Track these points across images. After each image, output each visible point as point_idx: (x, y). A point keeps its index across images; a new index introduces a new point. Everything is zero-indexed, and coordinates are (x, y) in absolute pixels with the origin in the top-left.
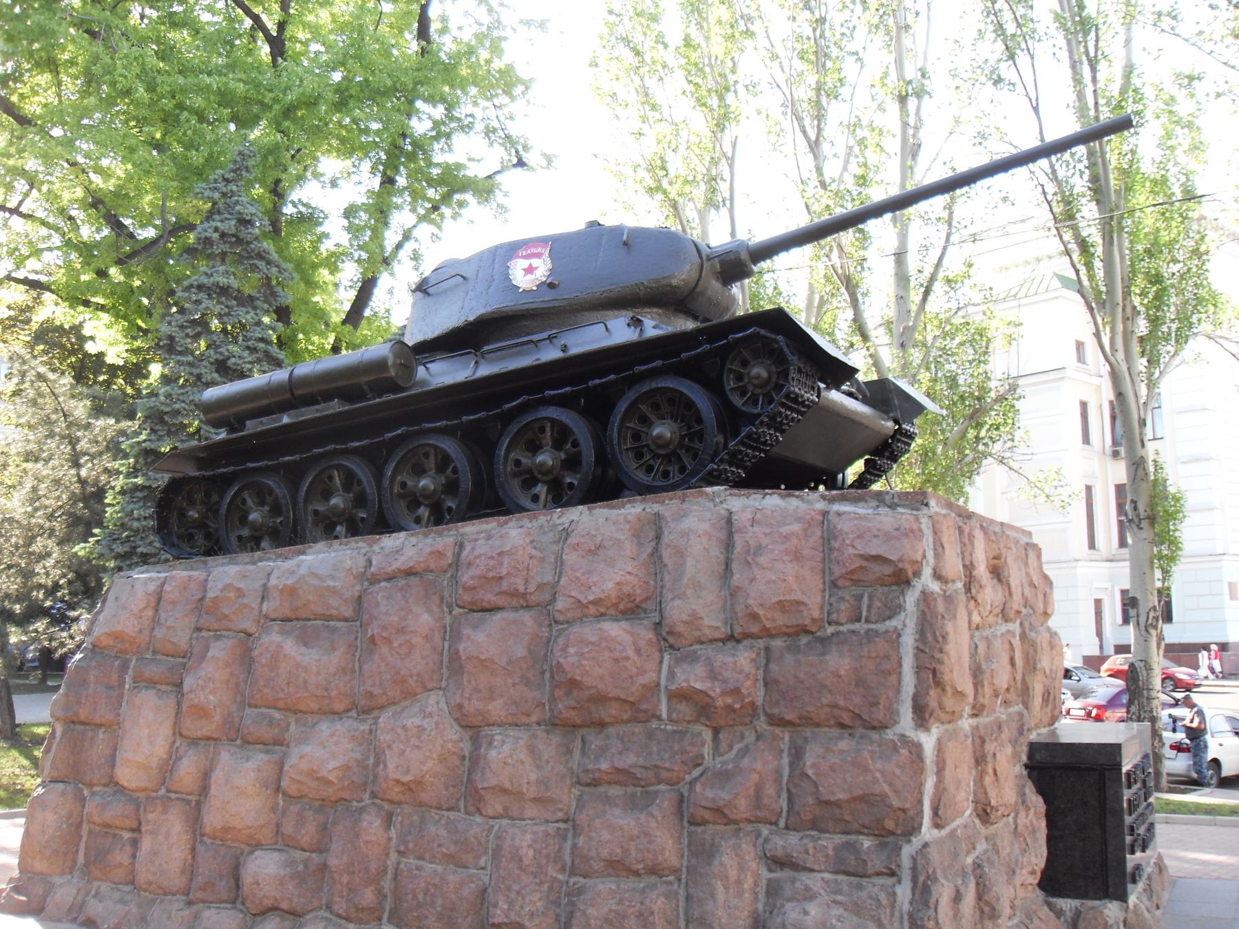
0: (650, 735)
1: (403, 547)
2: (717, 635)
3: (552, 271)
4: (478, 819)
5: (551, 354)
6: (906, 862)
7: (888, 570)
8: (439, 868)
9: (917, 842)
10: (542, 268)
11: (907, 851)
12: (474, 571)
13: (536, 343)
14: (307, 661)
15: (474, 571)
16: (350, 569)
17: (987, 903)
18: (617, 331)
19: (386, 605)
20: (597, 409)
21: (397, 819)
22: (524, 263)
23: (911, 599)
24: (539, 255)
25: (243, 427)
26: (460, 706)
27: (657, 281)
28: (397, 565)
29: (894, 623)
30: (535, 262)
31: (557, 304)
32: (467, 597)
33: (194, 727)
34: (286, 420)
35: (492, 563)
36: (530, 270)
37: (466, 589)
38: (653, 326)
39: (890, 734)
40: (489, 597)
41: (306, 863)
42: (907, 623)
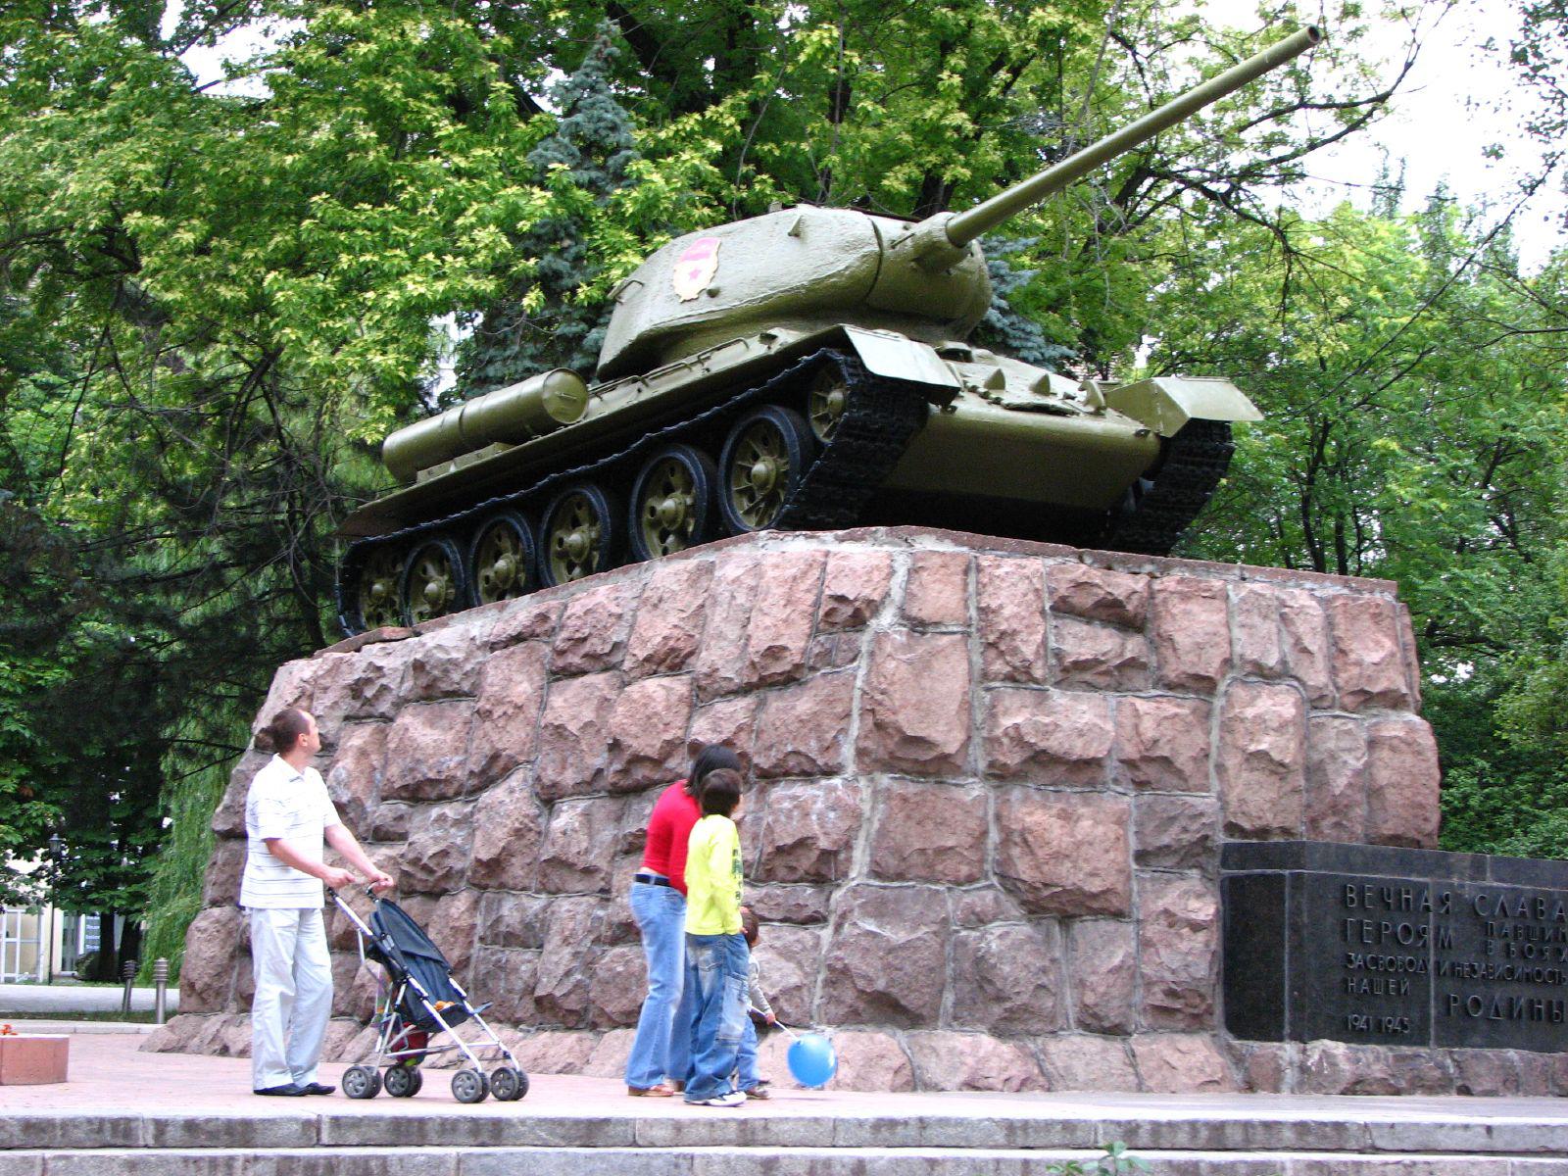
1: (522, 610)
2: (732, 686)
5: (697, 374)
12: (564, 634)
15: (564, 634)
16: (473, 639)
18: (751, 349)
25: (414, 480)
30: (700, 264)
31: (692, 320)
32: (560, 663)
34: (453, 469)
35: (579, 623)
36: (694, 275)
37: (561, 653)
40: (575, 659)
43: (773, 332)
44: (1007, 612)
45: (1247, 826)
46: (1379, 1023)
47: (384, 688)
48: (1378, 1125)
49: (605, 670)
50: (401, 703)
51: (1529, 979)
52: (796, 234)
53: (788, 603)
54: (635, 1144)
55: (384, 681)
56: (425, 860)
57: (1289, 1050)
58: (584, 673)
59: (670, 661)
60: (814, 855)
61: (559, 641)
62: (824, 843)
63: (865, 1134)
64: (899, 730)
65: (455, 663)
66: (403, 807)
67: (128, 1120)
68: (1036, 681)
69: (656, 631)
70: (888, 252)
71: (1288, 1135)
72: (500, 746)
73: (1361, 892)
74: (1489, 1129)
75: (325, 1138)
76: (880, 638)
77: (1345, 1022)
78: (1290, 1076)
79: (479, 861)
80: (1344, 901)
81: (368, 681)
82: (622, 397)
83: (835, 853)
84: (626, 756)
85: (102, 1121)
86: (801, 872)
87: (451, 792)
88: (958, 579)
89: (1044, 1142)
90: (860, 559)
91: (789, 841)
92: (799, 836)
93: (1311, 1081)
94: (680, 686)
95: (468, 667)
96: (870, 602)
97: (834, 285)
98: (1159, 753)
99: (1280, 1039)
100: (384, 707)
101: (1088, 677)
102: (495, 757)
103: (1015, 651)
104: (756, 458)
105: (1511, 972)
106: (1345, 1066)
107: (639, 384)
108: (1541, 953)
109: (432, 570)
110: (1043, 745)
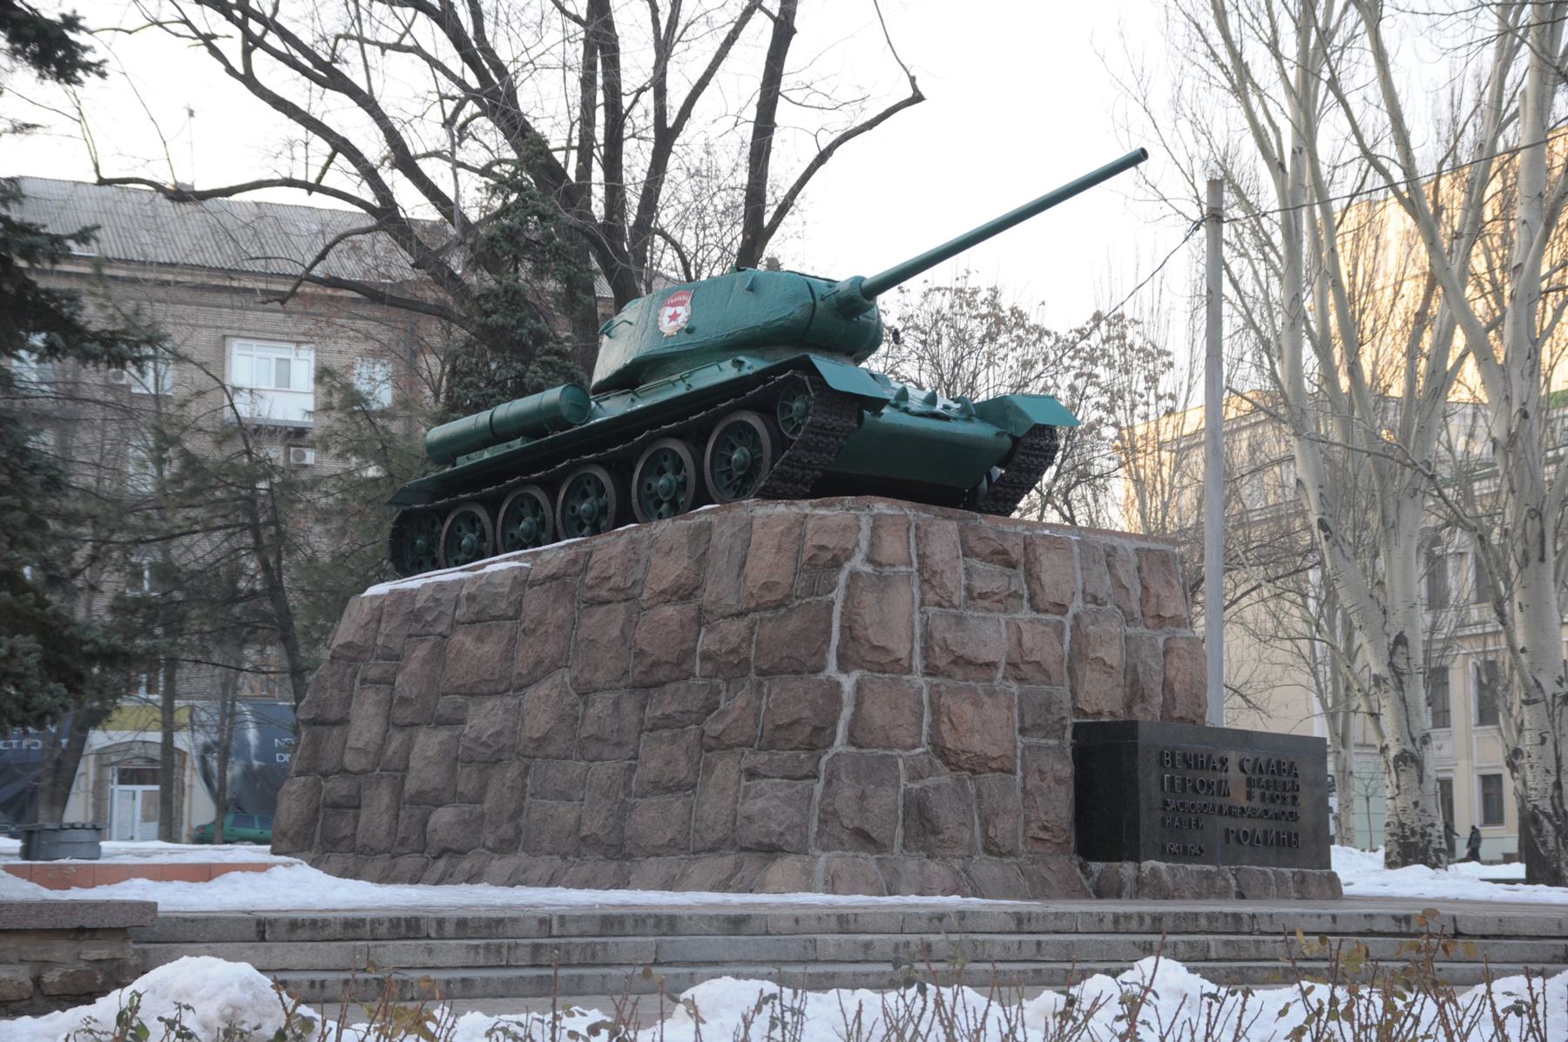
0: (688, 689)
2: (733, 611)
3: (690, 318)
4: (582, 763)
5: (680, 390)
6: (822, 766)
7: (830, 556)
8: (554, 803)
9: (831, 752)
10: (683, 312)
11: (825, 758)
12: (593, 574)
13: (673, 383)
14: (475, 651)
17: (929, 820)
18: (722, 372)
19: (534, 602)
20: (696, 437)
21: (532, 770)
22: (669, 311)
23: (842, 578)
24: (682, 303)
26: (576, 678)
27: (769, 323)
28: (546, 572)
29: (832, 595)
30: (680, 309)
32: (589, 595)
33: (402, 715)
36: (674, 317)
37: (591, 588)
38: (753, 365)
39: (821, 676)
41: (471, 813)
42: (838, 595)
43: (741, 358)
44: (937, 558)
45: (1088, 710)
46: (1185, 848)
47: (442, 613)
48: (1262, 915)
49: (626, 600)
50: (455, 624)
51: (1277, 817)
52: (751, 289)
53: (779, 549)
54: (767, 933)
55: (442, 609)
56: (484, 738)
57: (1127, 869)
58: (609, 602)
59: (683, 593)
60: (808, 730)
61: (589, 578)
62: (816, 723)
63: (923, 924)
64: (868, 641)
65: (502, 595)
66: (460, 699)
67: (417, 919)
68: (953, 606)
69: (670, 570)
70: (819, 304)
71: (1203, 923)
72: (543, 655)
73: (1173, 755)
74: (1334, 917)
75: (555, 932)
76: (854, 576)
77: (1164, 847)
78: (1129, 887)
79: (531, 739)
80: (1161, 764)
81: (428, 609)
82: (614, 407)
83: (823, 729)
84: (649, 661)
85: (399, 919)
86: (796, 743)
87: (502, 688)
88: (903, 534)
89: (1042, 929)
90: (829, 518)
91: (787, 721)
92: (795, 717)
93: (1141, 888)
94: (690, 610)
95: (512, 598)
96: (845, 550)
97: (781, 326)
98: (1034, 658)
99: (1120, 860)
100: (442, 628)
101: (986, 603)
102: (539, 663)
103: (943, 585)
104: (733, 448)
105: (1266, 812)
106: (1166, 878)
107: (631, 396)
108: (1284, 799)
109: (464, 530)
110: (961, 652)
